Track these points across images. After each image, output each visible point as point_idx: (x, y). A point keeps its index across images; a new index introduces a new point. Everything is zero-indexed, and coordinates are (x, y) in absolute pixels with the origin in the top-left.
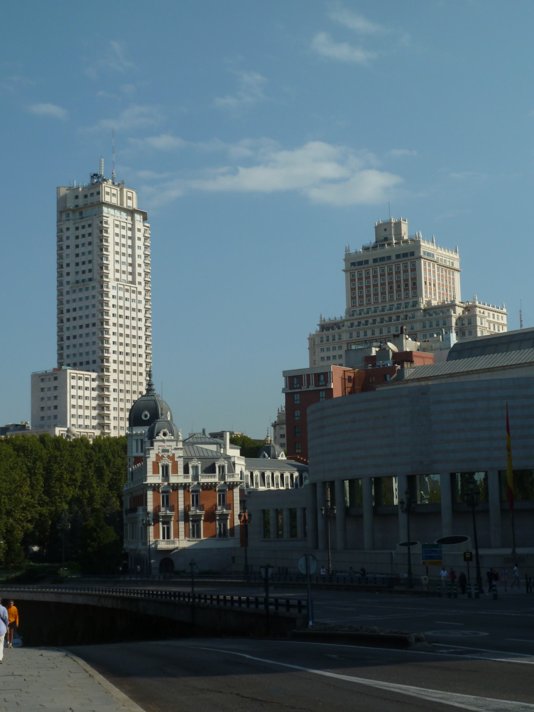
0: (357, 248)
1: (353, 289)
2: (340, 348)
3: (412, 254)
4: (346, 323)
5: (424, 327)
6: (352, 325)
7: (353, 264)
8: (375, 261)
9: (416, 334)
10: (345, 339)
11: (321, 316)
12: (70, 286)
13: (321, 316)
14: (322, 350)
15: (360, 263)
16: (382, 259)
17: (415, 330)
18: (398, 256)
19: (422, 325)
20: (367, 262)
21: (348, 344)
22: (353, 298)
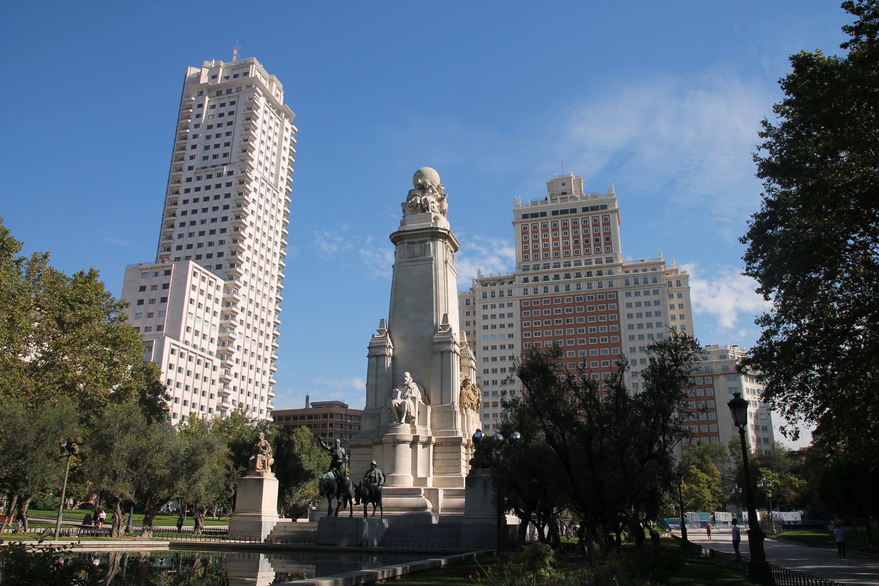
2: (510, 305)
3: (604, 207)
4: (517, 278)
5: (627, 283)
6: (526, 280)
7: (525, 216)
8: (555, 213)
9: (617, 292)
10: (517, 295)
12: (194, 170)
14: (485, 307)
15: (534, 215)
16: (564, 212)
18: (585, 209)
19: (624, 282)
20: (544, 214)
21: (521, 301)
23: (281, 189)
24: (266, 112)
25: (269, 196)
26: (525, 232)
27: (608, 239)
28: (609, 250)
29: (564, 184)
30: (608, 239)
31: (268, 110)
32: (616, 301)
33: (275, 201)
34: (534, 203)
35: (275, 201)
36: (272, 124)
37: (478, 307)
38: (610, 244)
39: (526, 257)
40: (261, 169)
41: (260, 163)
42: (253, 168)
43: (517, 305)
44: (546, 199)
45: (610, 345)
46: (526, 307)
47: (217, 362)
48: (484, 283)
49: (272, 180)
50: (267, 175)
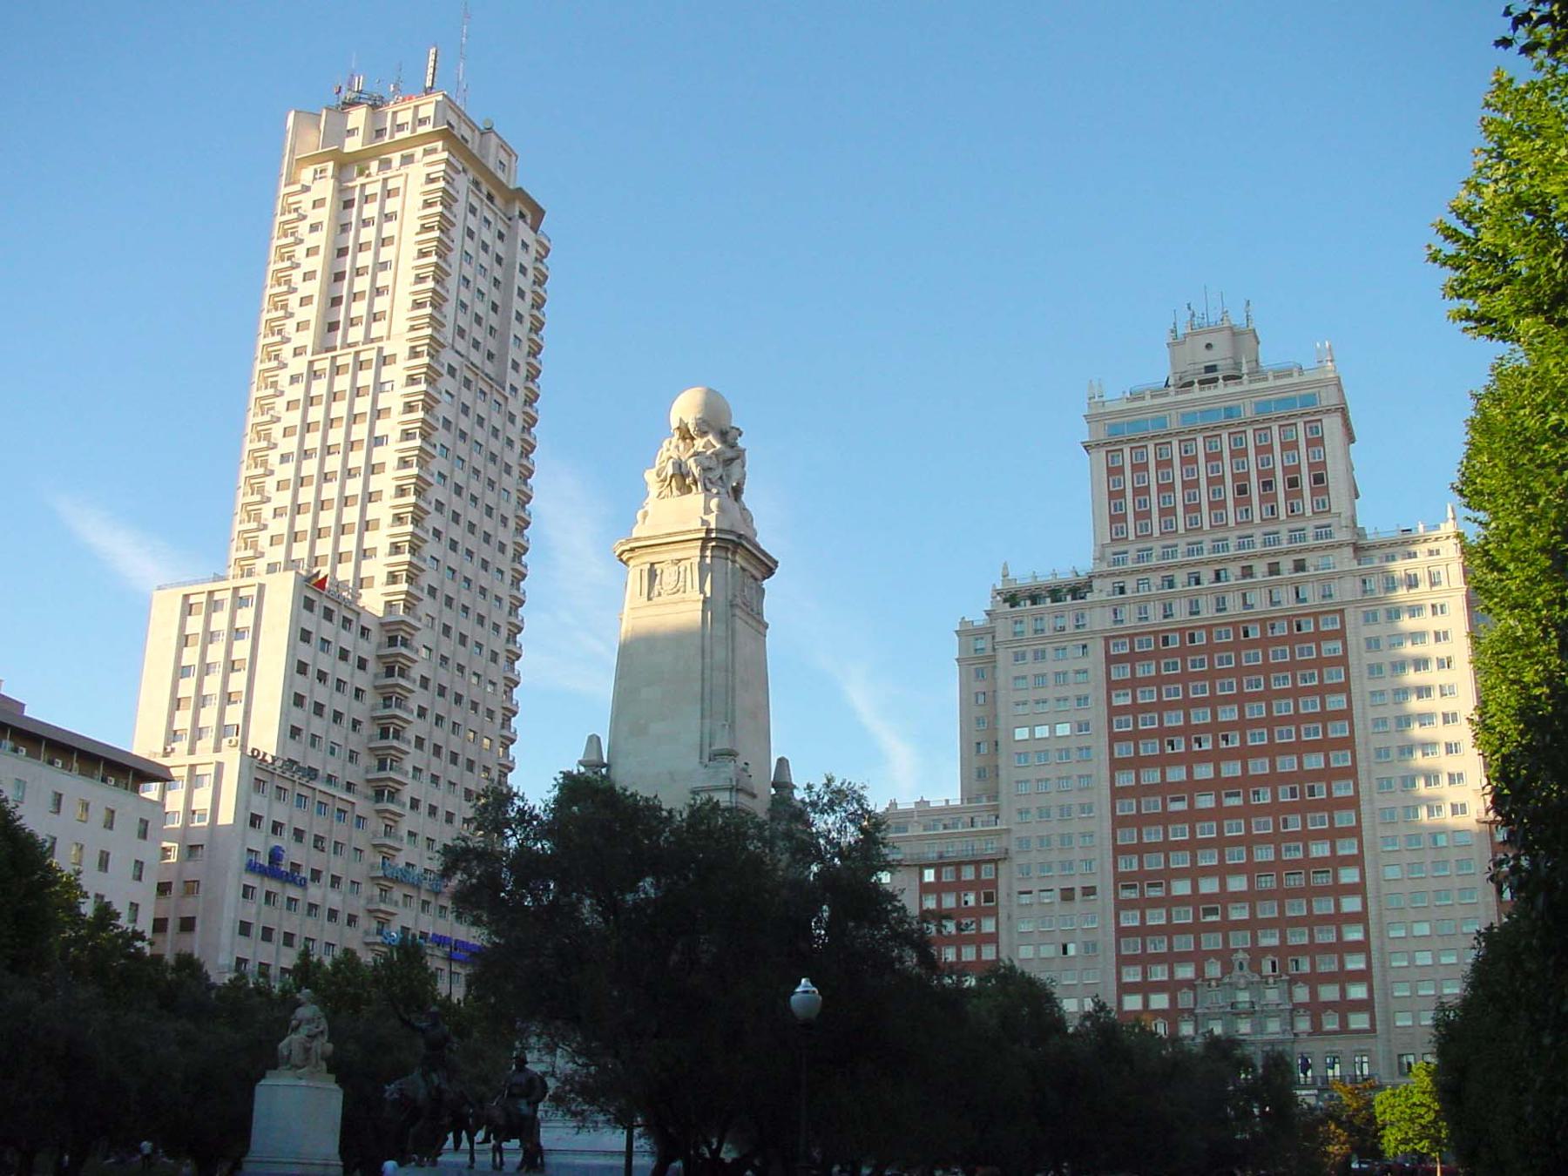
0: (1115, 393)
1: (1116, 495)
4: (1096, 584)
9: (1342, 611)
11: (1005, 567)
13: (1005, 567)
17: (1337, 598)
21: (1107, 639)
22: (1117, 519)
23: (513, 389)
24: (473, 210)
25: (481, 408)
26: (1114, 471)
27: (1319, 479)
28: (1323, 509)
29: (1209, 346)
30: (1319, 479)
31: (476, 204)
32: (1340, 635)
33: (497, 420)
34: (1136, 396)
35: (497, 420)
36: (488, 236)
37: (1004, 657)
38: (1326, 490)
39: (1120, 531)
40: (461, 345)
41: (461, 332)
42: (443, 346)
43: (1097, 648)
44: (1167, 385)
45: (1326, 746)
46: (1122, 654)
47: (363, 807)
48: (1012, 599)
49: (489, 368)
50: (476, 357)
